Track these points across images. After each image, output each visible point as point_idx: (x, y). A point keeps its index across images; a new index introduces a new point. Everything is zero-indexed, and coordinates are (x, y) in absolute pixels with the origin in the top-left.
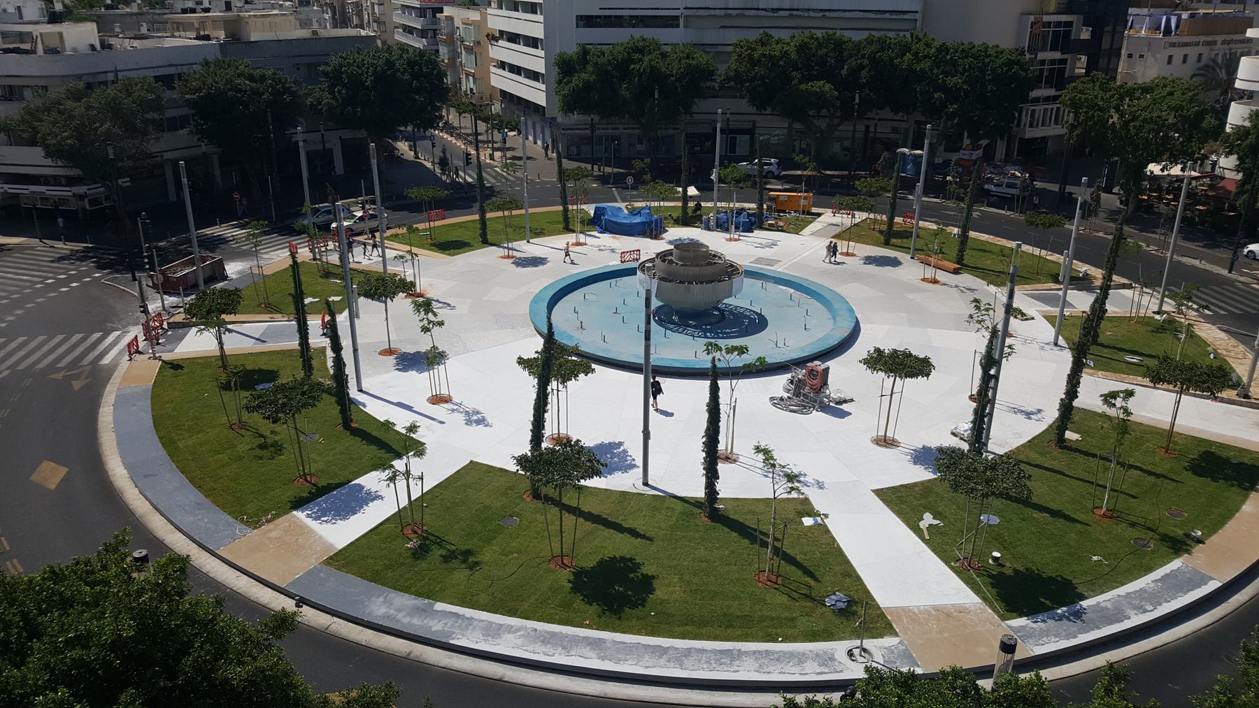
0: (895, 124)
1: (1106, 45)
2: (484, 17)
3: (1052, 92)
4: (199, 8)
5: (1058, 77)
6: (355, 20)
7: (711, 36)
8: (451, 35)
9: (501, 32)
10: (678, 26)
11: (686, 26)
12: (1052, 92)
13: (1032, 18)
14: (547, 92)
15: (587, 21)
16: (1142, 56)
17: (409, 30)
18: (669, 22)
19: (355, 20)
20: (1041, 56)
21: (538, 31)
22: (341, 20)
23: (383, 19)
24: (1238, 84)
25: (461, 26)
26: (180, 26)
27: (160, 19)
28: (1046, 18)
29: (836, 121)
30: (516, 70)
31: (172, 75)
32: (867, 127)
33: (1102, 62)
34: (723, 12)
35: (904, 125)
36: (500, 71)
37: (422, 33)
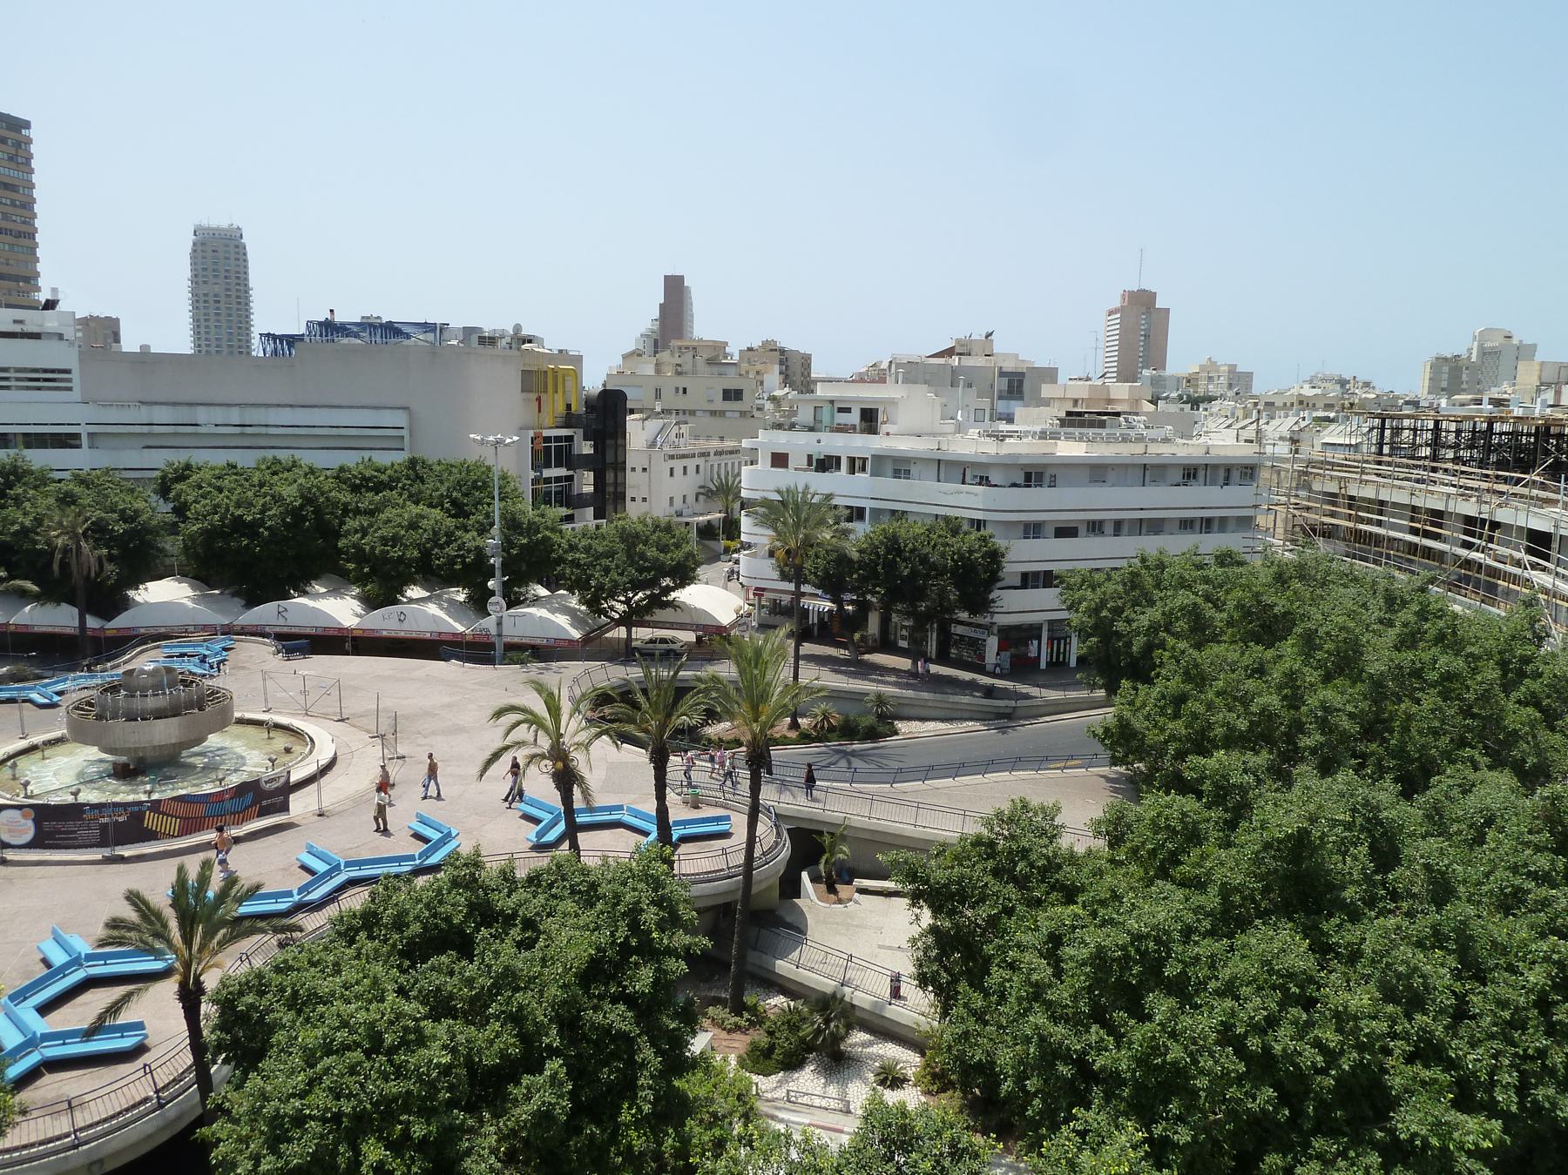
1: (610, 458)
10: (79, 447)
13: (531, 433)
18: (66, 441)
20: (547, 473)
28: (546, 433)
33: (610, 477)
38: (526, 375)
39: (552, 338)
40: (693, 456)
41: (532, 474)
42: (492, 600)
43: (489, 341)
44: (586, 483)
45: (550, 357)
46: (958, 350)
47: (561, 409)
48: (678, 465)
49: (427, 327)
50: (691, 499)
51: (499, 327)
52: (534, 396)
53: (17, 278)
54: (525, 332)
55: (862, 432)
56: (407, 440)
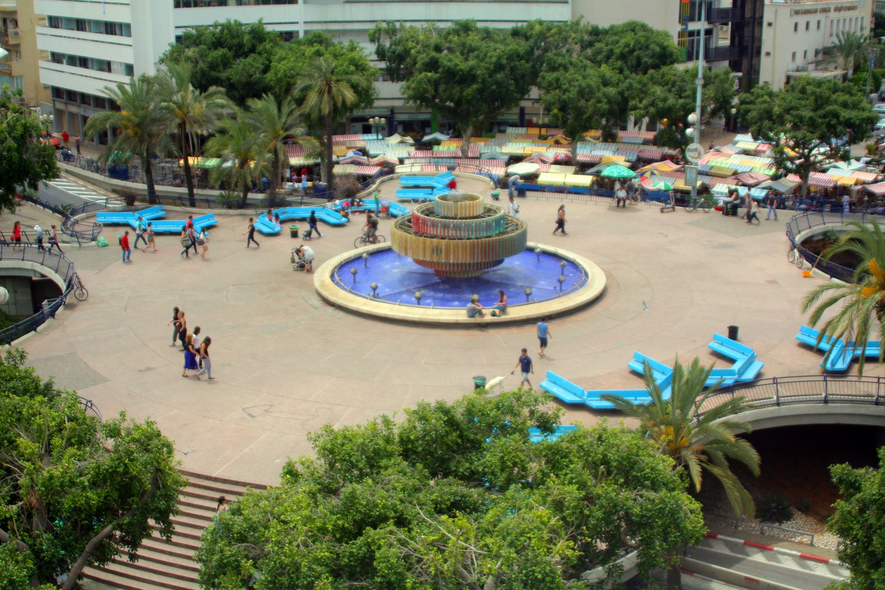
1: (748, 14)
40: (815, 11)
41: (679, 28)
42: (692, 146)
44: (723, 39)
48: (802, 20)
50: (811, 56)
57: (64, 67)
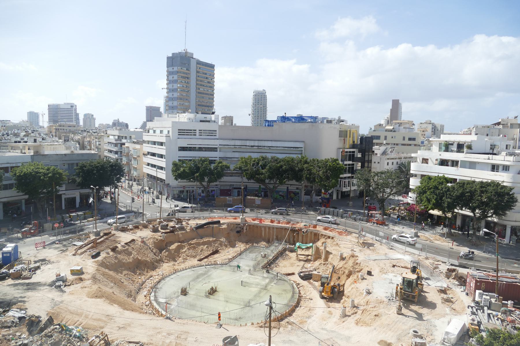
0: (297, 186)
1: (366, 159)
2: (142, 148)
3: (350, 175)
4: (22, 141)
5: (352, 170)
6: (88, 147)
7: (229, 155)
8: (128, 153)
9: (148, 153)
10: (217, 151)
11: (220, 151)
12: (350, 175)
13: (341, 150)
14: (166, 174)
15: (182, 149)
16: (379, 163)
17: (110, 151)
18: (214, 149)
19: (88, 147)
20: (346, 163)
21: (163, 152)
22: (83, 147)
23: (100, 147)
24: (411, 172)
25: (132, 150)
26: (13, 148)
27: (5, 145)
28: (346, 150)
29: (276, 185)
30: (153, 166)
31: (8, 167)
32: (288, 187)
33: (366, 165)
34: (233, 147)
35: (300, 187)
36: (148, 167)
37: (116, 153)
38: (341, 132)
39: (350, 120)
40: (396, 159)
43: (329, 122)
45: (349, 126)
46: (502, 123)
47: (351, 142)
49: (311, 117)
51: (333, 117)
52: (343, 138)
53: (208, 106)
54: (341, 119)
55: (457, 152)
56: (303, 152)
57: (150, 167)
